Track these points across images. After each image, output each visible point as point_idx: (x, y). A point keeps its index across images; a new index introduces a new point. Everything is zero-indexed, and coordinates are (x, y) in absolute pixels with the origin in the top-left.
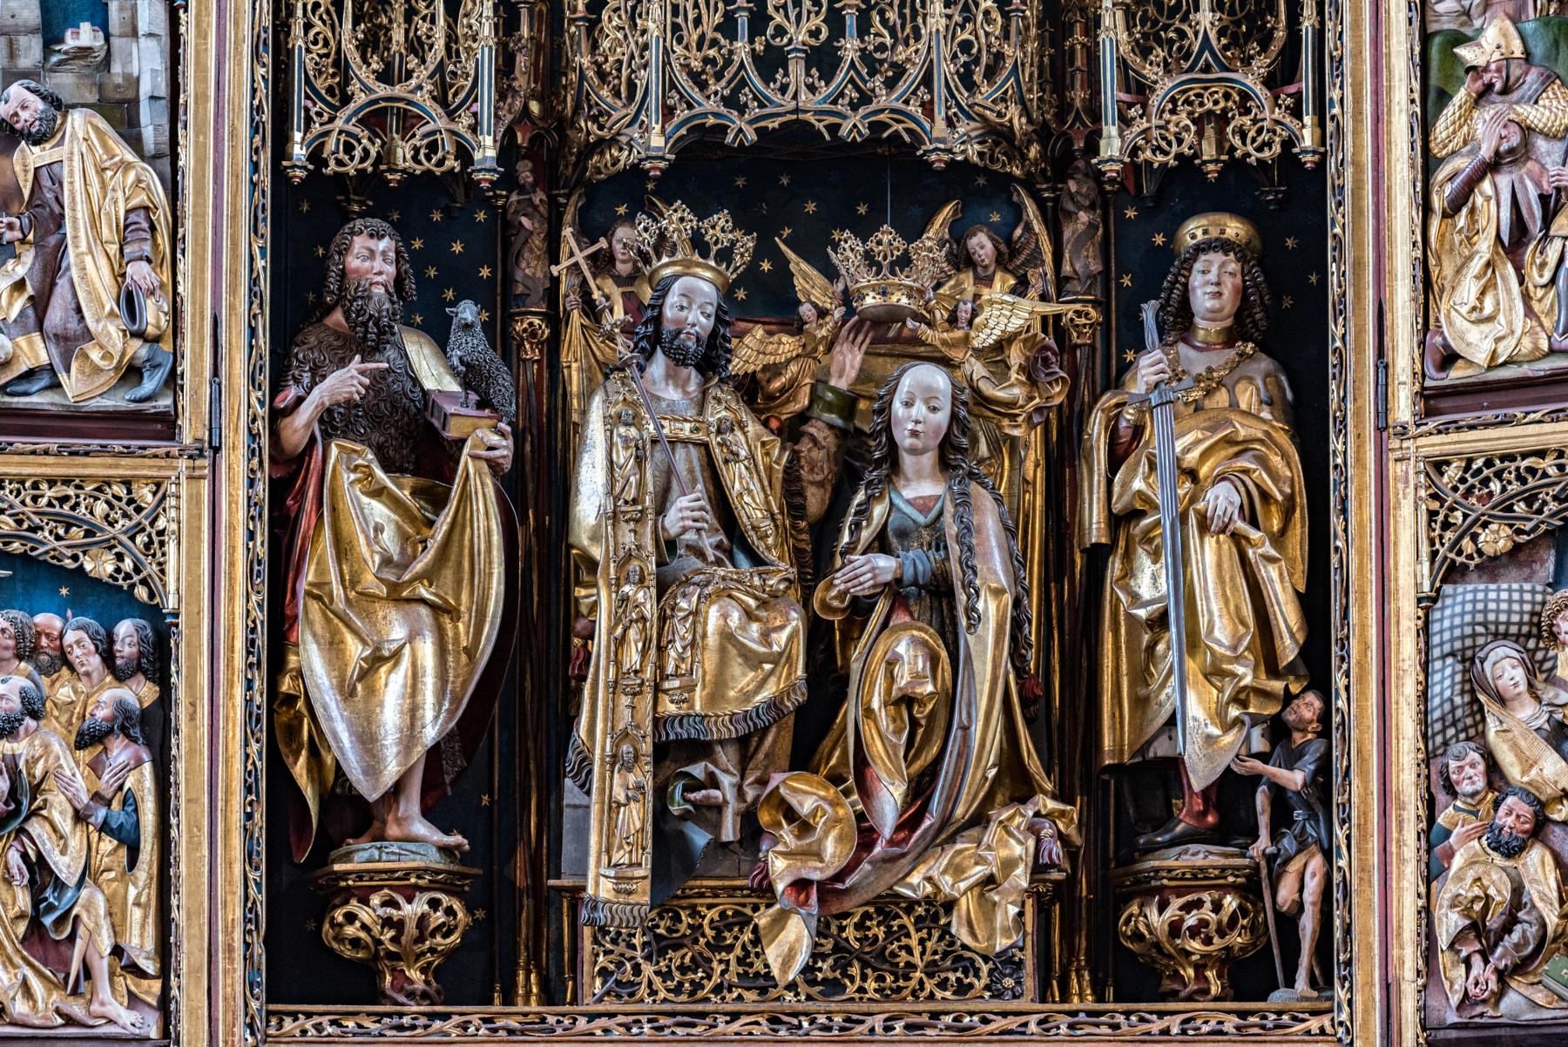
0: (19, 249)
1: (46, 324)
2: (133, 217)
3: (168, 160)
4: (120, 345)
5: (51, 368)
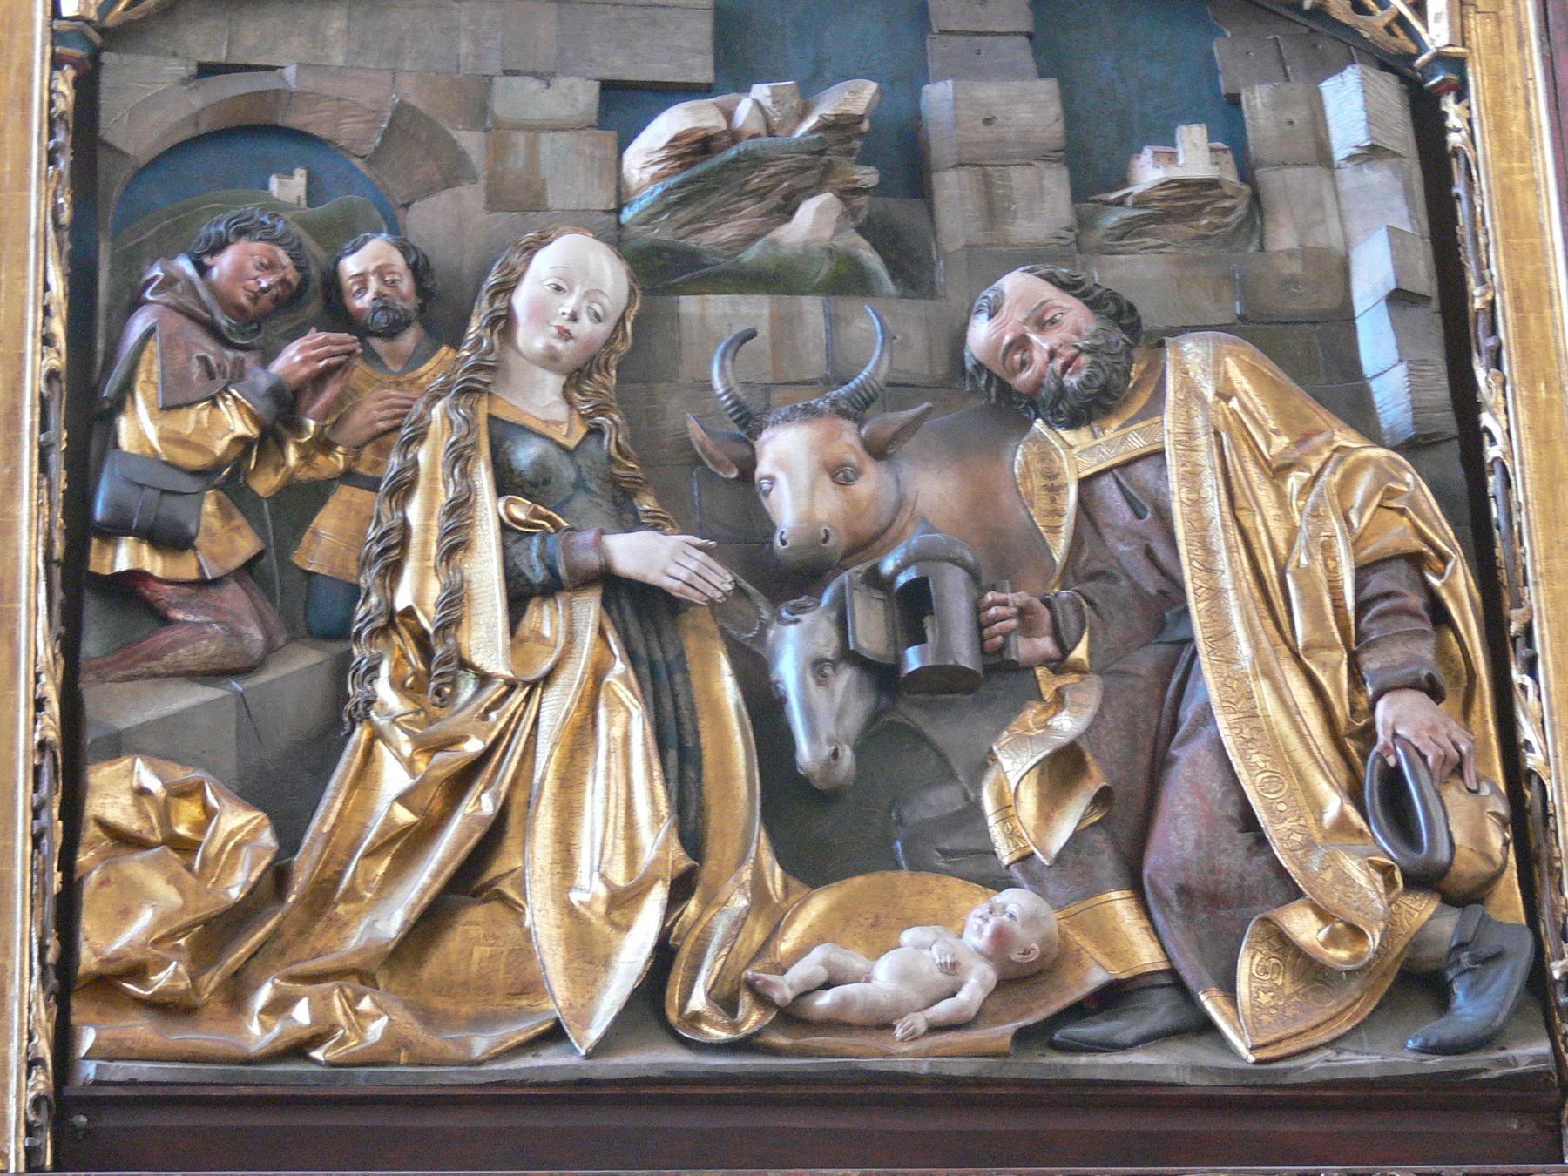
0: (1048, 684)
1: (1153, 861)
2: (1377, 583)
3: (1454, 448)
4: (1379, 905)
5: (1174, 980)
